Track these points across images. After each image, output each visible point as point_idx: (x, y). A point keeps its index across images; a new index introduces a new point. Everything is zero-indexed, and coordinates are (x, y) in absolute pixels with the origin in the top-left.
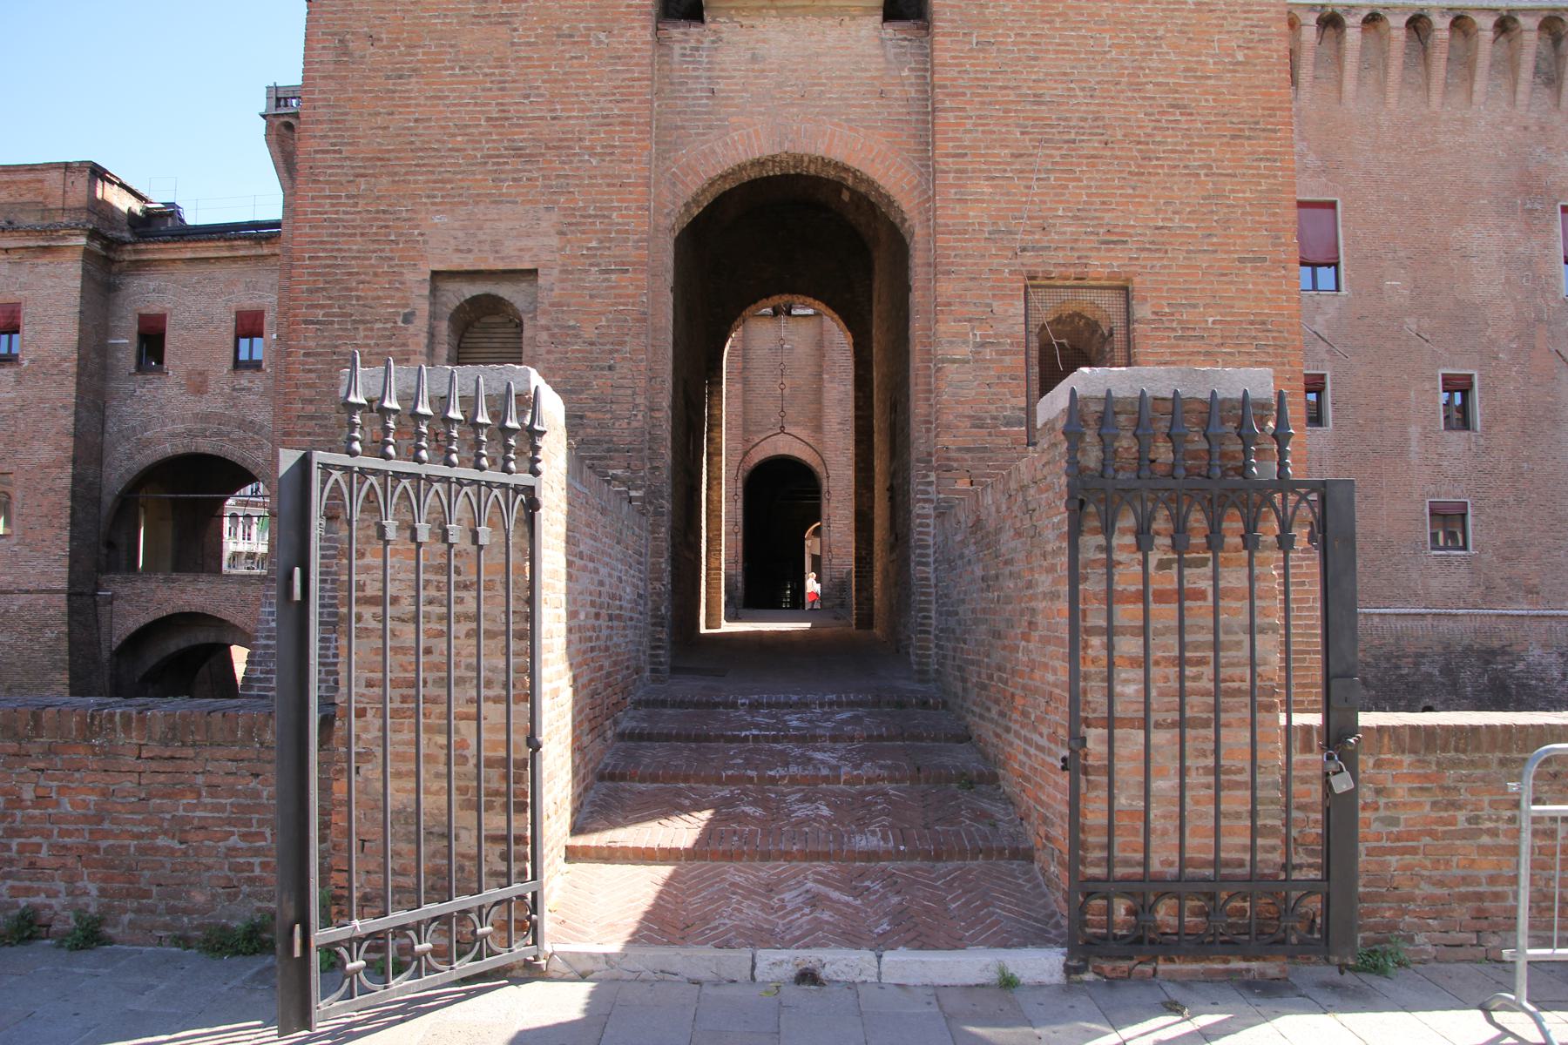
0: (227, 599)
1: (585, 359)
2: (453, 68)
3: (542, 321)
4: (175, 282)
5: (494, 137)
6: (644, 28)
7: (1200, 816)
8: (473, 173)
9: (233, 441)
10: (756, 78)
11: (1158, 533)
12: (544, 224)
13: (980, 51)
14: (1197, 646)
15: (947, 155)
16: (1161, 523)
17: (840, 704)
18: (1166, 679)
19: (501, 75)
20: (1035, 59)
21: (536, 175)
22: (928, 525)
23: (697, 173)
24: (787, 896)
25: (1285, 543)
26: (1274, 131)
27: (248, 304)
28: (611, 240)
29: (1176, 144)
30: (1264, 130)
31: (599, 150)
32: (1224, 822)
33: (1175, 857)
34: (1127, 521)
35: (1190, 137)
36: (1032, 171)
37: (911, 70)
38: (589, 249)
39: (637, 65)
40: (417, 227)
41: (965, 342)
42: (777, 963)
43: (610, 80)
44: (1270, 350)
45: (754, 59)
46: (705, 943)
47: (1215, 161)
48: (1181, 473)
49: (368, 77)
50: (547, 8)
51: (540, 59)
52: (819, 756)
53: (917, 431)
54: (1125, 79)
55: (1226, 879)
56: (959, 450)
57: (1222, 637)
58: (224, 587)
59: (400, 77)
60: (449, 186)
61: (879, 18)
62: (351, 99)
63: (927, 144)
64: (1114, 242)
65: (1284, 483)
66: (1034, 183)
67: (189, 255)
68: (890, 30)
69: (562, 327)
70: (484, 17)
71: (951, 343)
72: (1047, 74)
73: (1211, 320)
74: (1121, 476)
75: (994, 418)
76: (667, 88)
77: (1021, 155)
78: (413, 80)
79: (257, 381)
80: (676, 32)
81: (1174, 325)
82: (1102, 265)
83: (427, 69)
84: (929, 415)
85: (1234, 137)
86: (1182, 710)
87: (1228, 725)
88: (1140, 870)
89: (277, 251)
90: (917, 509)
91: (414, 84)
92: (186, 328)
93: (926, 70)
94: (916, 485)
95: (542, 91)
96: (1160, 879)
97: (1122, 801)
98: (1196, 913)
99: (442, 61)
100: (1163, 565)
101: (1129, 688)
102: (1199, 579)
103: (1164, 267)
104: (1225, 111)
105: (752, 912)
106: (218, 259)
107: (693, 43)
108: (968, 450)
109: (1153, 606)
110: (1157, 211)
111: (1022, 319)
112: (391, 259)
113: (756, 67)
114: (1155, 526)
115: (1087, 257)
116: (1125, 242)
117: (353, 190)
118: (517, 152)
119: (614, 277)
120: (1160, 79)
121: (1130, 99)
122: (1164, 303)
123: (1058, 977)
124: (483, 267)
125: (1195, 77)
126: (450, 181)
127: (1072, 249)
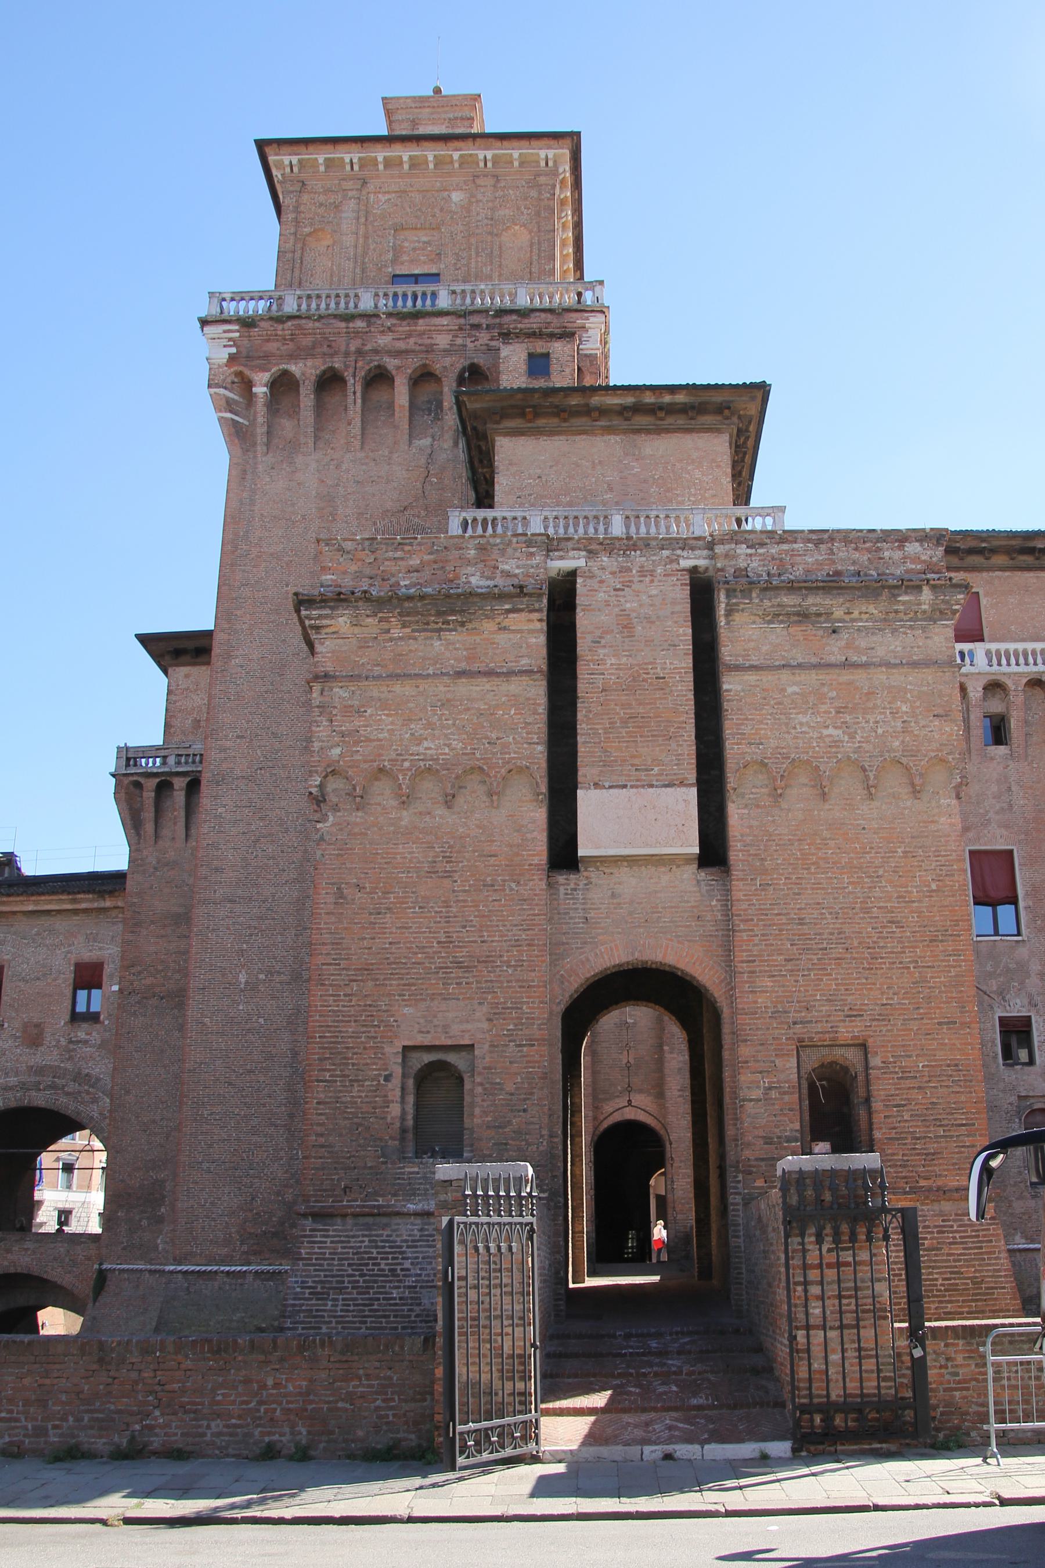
0: (55, 1259)
1: (508, 1105)
2: (414, 908)
3: (478, 1079)
4: (15, 933)
5: (443, 955)
6: (541, 880)
7: (854, 1372)
8: (430, 979)
9: (68, 1094)
10: (615, 908)
11: (827, 1235)
12: (478, 1014)
13: (763, 890)
14: (848, 1289)
15: (742, 962)
16: (828, 1230)
17: (683, 1333)
18: (834, 1306)
19: (447, 912)
20: (799, 894)
21: (471, 980)
22: (738, 1210)
23: (578, 975)
24: (656, 1427)
25: (886, 1238)
26: (959, 936)
27: (88, 955)
28: (523, 1024)
29: (893, 947)
31: (513, 963)
32: (864, 1375)
33: (842, 1393)
34: (812, 1230)
35: (902, 942)
36: (799, 970)
37: (718, 900)
38: (508, 1030)
39: (537, 905)
40: (393, 1016)
41: (758, 1087)
42: (652, 1452)
43: (519, 915)
45: (613, 895)
46: (618, 1444)
47: (920, 957)
48: (835, 1206)
49: (357, 914)
50: (476, 867)
51: (472, 901)
52: (670, 1362)
53: (730, 1146)
55: (867, 1402)
56: (757, 1159)
57: (859, 1284)
58: (52, 1246)
59: (379, 914)
60: (413, 988)
61: (696, 866)
62: (346, 929)
63: (730, 951)
65: (884, 1210)
66: (800, 978)
67: (31, 908)
68: (702, 874)
69: (492, 1083)
70: (434, 873)
71: (749, 1088)
72: (806, 904)
74: (808, 1208)
75: (779, 1137)
76: (556, 917)
77: (791, 960)
78: (388, 915)
79: (94, 1034)
80: (561, 879)
82: (846, 1031)
83: (396, 908)
84: (736, 1135)
86: (841, 1320)
87: (864, 1327)
88: (825, 1400)
89: (120, 904)
90: (731, 1199)
92: (23, 980)
93: (728, 900)
94: (730, 1183)
95: (474, 923)
96: (836, 1403)
97: (815, 1366)
98: (853, 1420)
99: (407, 903)
100: (829, 1250)
101: (816, 1311)
102: (847, 1257)
103: (888, 1031)
104: (925, 923)
105: (639, 1433)
106: (59, 912)
107: (572, 886)
108: (763, 1160)
109: (826, 1271)
110: (883, 993)
111: (796, 1070)
112: (376, 1038)
113: (615, 901)
114: (825, 1232)
117: (348, 991)
118: (459, 965)
119: (525, 1049)
120: (882, 904)
121: (861, 918)
122: (890, 1055)
123: (789, 1454)
124: (437, 1043)
125: (906, 902)
126: (414, 985)
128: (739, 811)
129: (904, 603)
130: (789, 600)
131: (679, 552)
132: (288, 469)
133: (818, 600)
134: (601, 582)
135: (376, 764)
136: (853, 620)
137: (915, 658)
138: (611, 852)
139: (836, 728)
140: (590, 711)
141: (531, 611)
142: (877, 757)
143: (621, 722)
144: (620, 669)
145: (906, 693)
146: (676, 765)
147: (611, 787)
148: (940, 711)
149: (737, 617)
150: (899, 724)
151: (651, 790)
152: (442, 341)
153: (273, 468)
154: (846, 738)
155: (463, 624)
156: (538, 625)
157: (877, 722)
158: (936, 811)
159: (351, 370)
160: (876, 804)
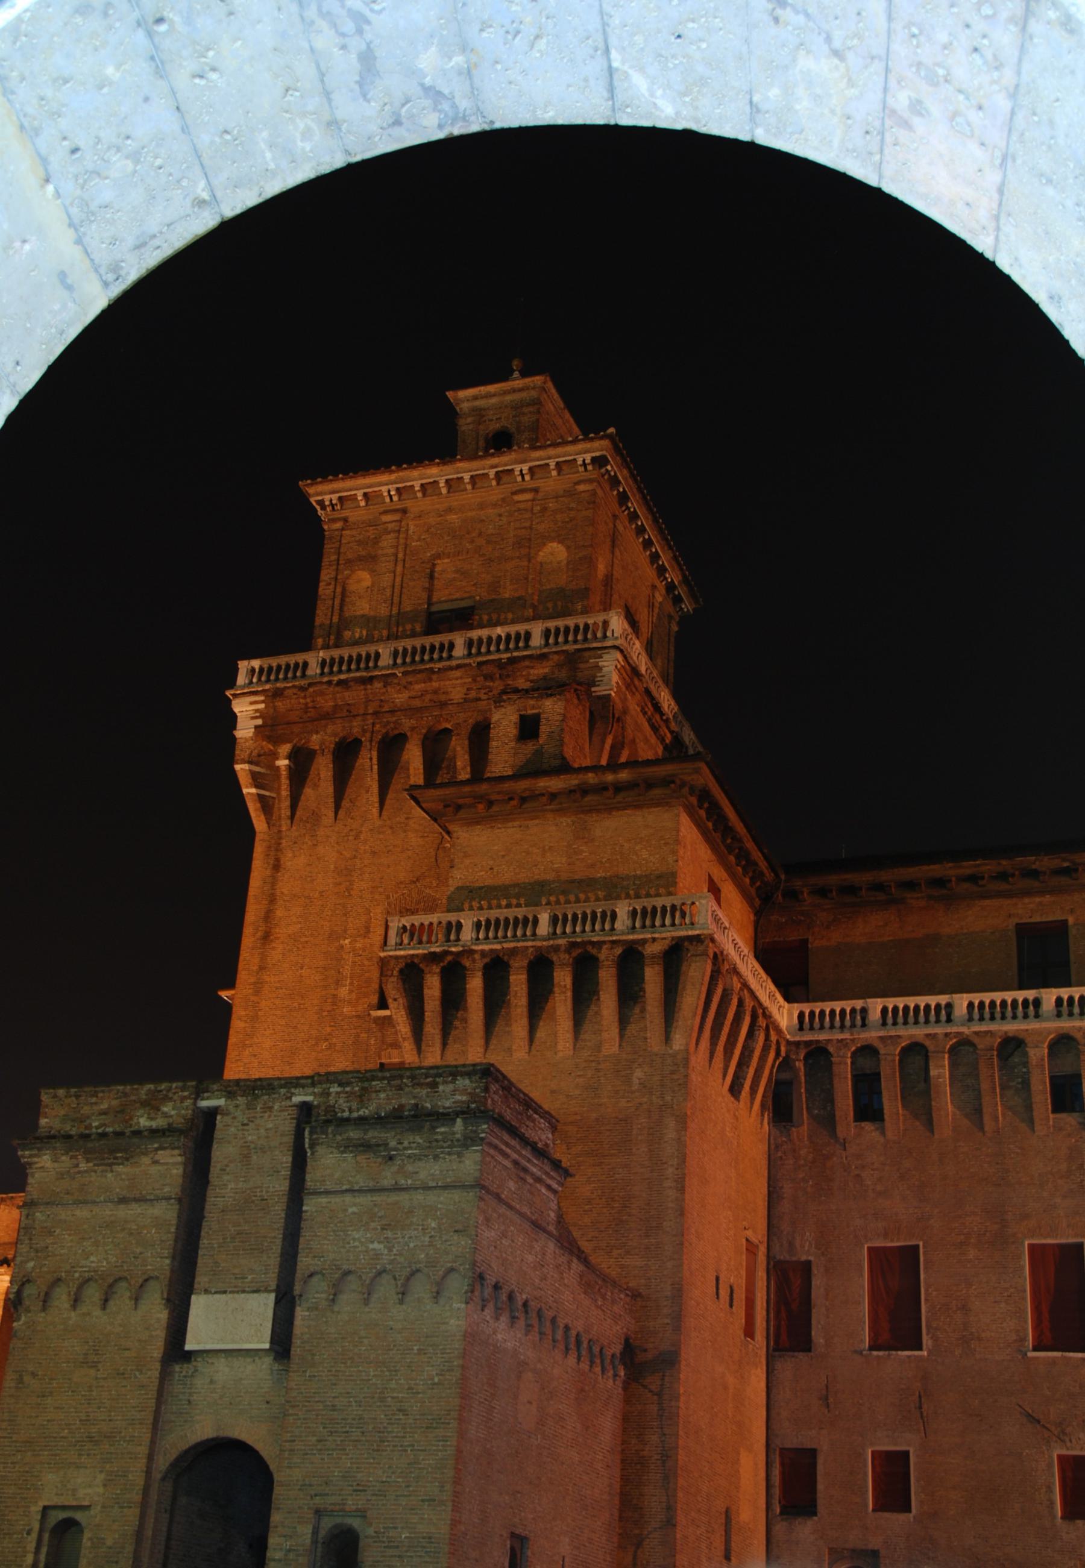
20: (335, 1384)
29: (398, 1432)
30: (443, 1423)
38: (116, 1494)
40: (40, 1480)
44: (432, 1554)
54: (377, 1396)
64: (360, 1491)
66: (326, 1457)
68: (276, 1366)
69: (97, 1538)
71: (275, 1549)
73: (403, 1536)
81: (385, 1539)
85: (427, 1428)
91: (49, 1400)
107: (184, 1373)
115: (346, 1499)
116: (365, 1491)
118: (91, 1439)
120: (395, 1395)
121: (378, 1406)
122: (381, 1526)
127: (340, 1495)
128: (303, 1313)
129: (442, 1133)
130: (354, 1134)
131: (293, 1090)
132: (310, 843)
133: (376, 1134)
134: (234, 1118)
135: (55, 1275)
136: (405, 1149)
137: (448, 1180)
138: (209, 1347)
139: (379, 1242)
140: (210, 1229)
141: (173, 1149)
142: (406, 1267)
143: (231, 1238)
144: (236, 1193)
145: (436, 1212)
146: (265, 1274)
147: (216, 1293)
148: (459, 1227)
149: (321, 1150)
150: (427, 1239)
151: (243, 1295)
152: (457, 694)
153: (295, 843)
154: (386, 1252)
155: (127, 1159)
156: (180, 1159)
157: (411, 1237)
158: (448, 1314)
159: (368, 735)
160: (404, 1307)
